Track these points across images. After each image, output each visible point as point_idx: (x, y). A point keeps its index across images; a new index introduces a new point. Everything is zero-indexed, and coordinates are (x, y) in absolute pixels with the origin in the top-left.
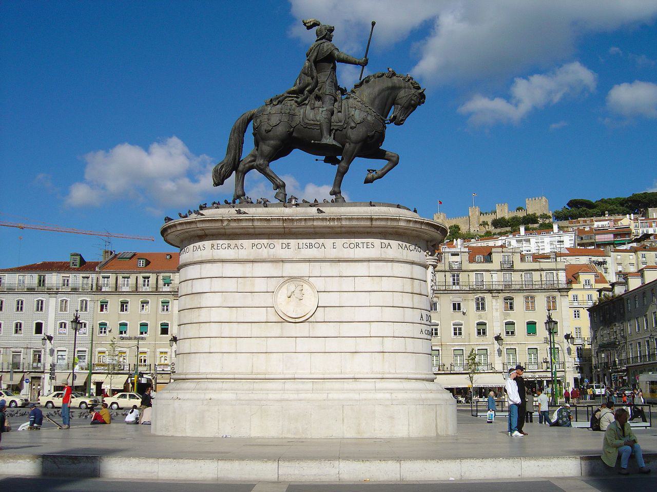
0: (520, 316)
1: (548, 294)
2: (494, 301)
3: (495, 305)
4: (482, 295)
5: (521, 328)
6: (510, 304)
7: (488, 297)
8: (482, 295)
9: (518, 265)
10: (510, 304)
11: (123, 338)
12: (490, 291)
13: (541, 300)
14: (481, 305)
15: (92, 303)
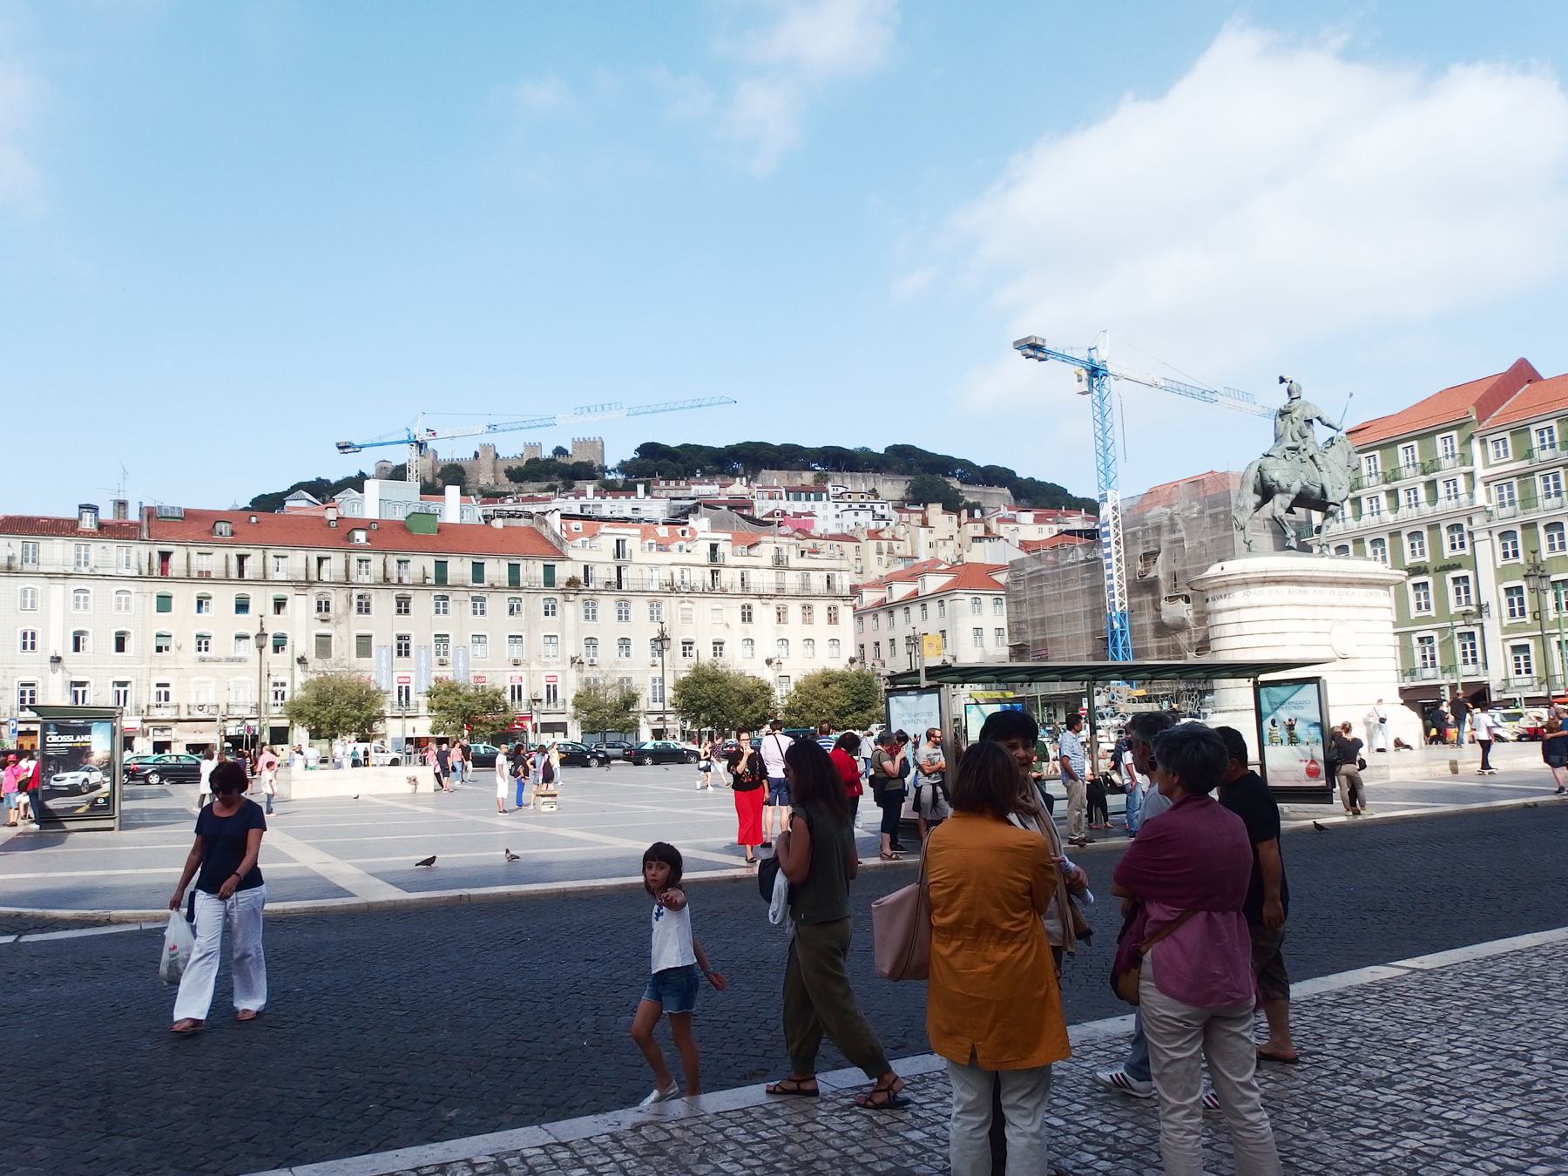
0: (795, 626)
1: (829, 603)
2: (764, 609)
3: (764, 613)
4: (748, 601)
5: (796, 645)
6: (781, 615)
7: (756, 604)
8: (748, 601)
9: (795, 561)
10: (781, 615)
11: (203, 660)
12: (760, 596)
13: (820, 608)
14: (747, 616)
15: (140, 597)
